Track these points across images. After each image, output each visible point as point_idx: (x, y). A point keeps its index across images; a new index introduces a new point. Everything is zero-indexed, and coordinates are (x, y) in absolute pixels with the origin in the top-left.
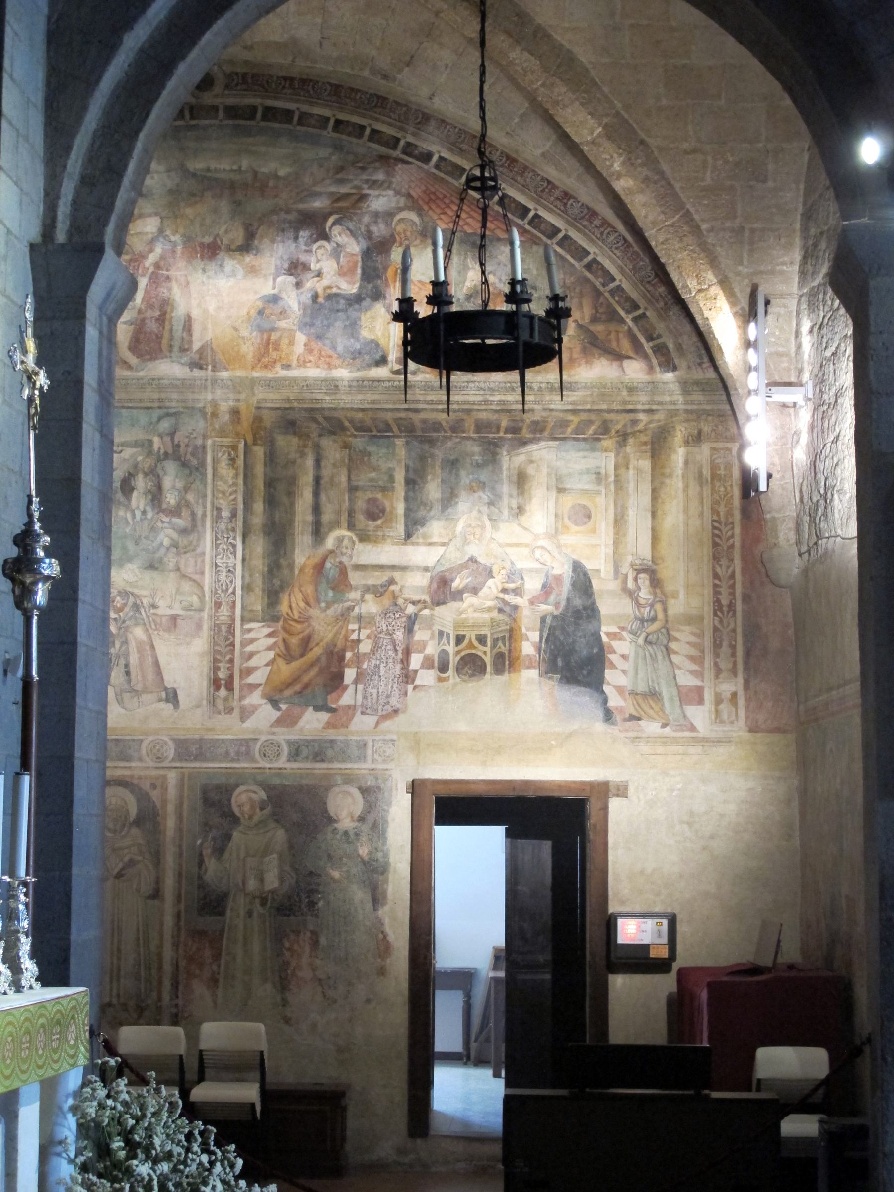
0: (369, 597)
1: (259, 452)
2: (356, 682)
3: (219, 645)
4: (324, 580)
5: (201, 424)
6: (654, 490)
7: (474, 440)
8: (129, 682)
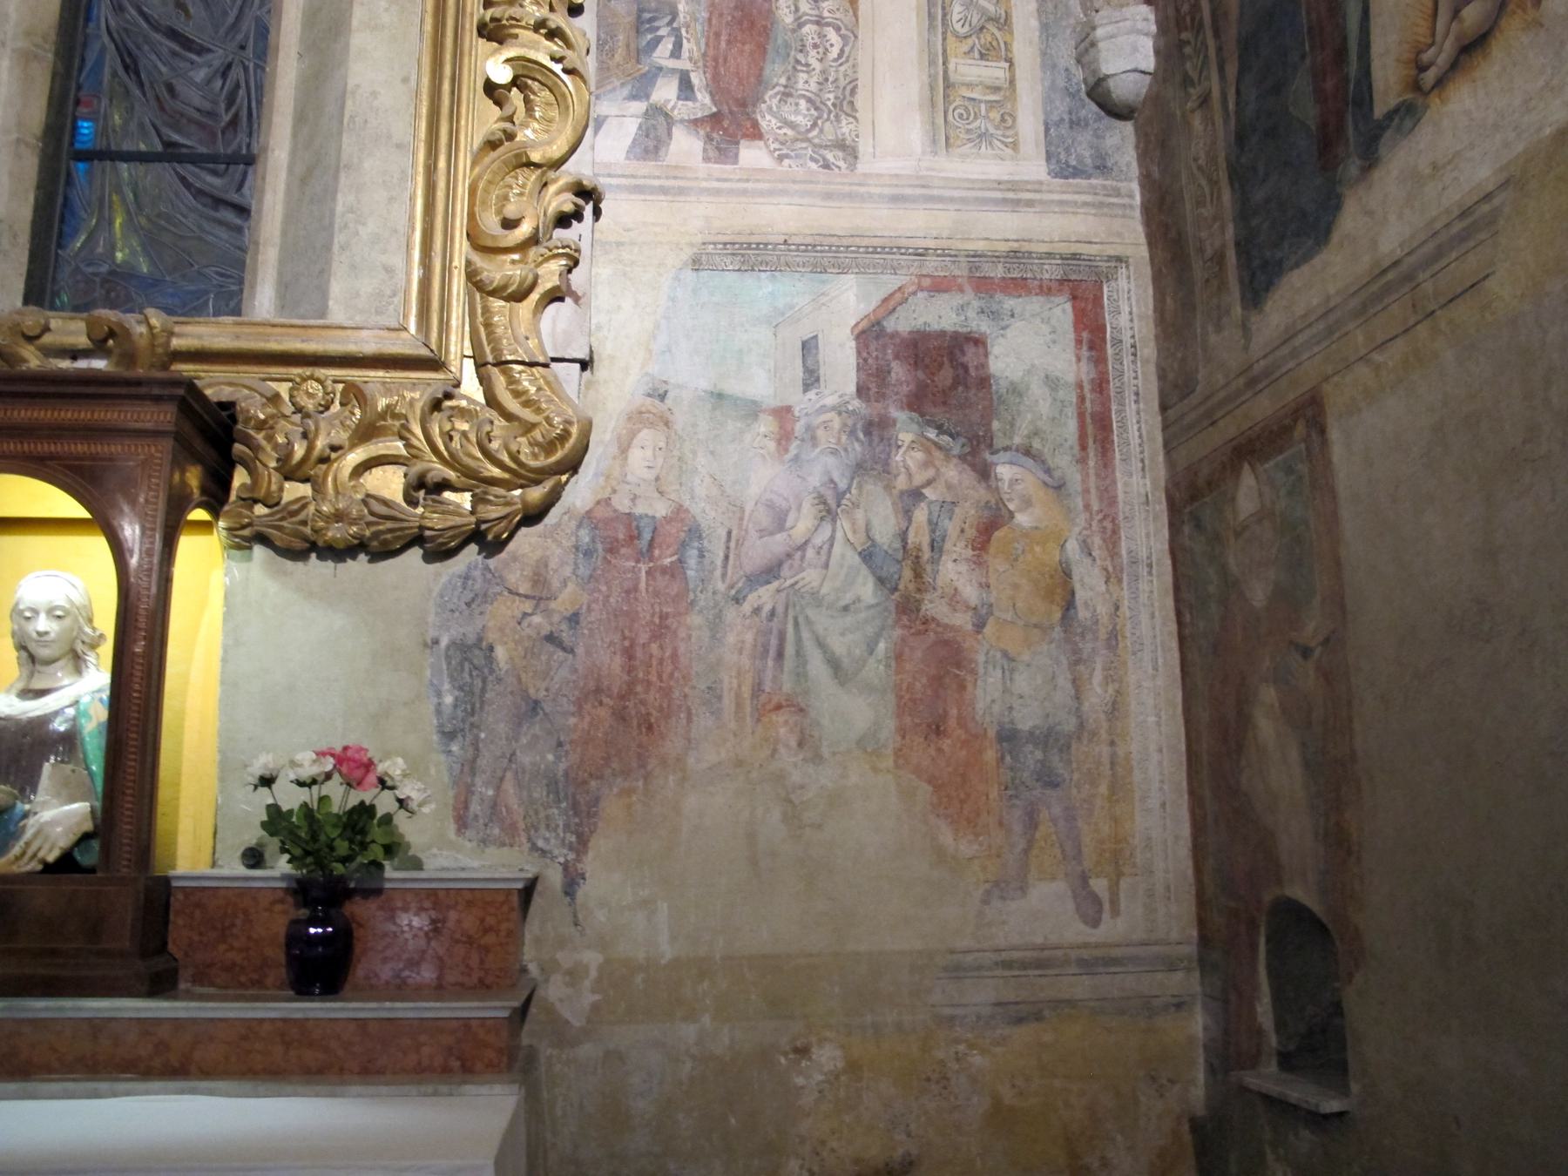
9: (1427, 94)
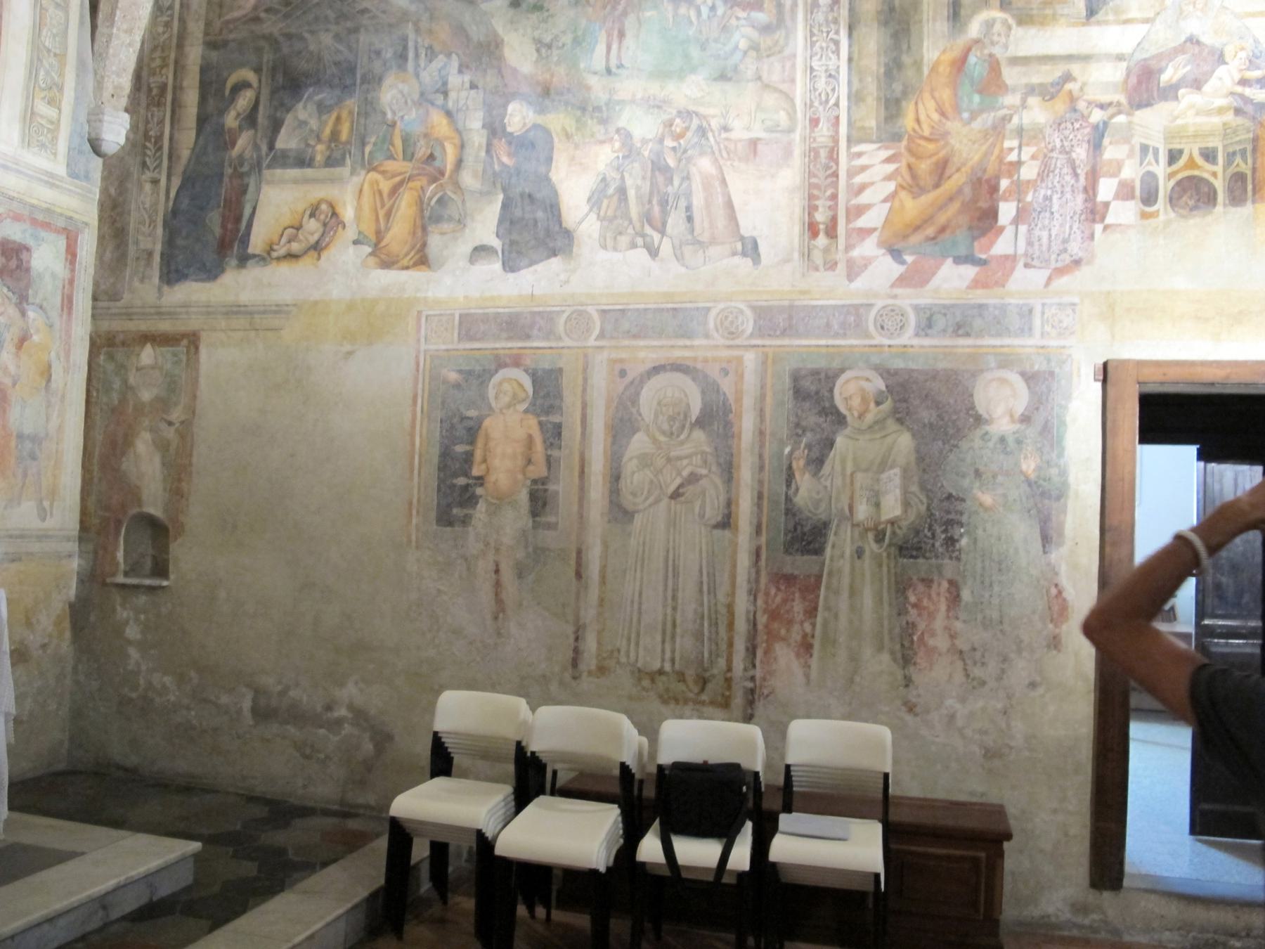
0: (1033, 101)
2: (1016, 221)
3: (815, 176)
8: (692, 231)
9: (272, 259)
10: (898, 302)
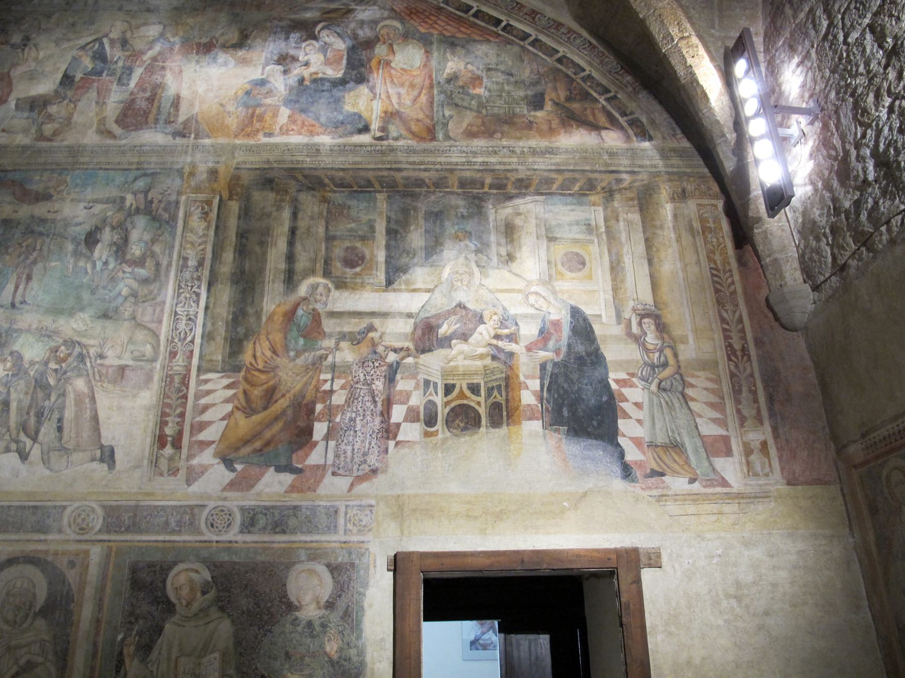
1: (234, 206)
2: (327, 438)
3: (169, 397)
4: (295, 329)
5: (178, 182)
6: (647, 240)
7: (459, 194)
8: (61, 439)
10: (226, 503)
